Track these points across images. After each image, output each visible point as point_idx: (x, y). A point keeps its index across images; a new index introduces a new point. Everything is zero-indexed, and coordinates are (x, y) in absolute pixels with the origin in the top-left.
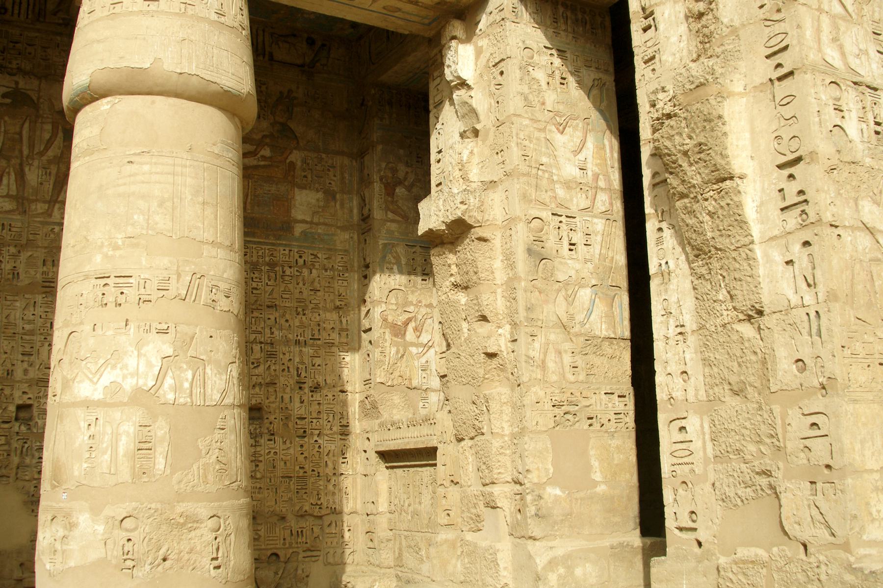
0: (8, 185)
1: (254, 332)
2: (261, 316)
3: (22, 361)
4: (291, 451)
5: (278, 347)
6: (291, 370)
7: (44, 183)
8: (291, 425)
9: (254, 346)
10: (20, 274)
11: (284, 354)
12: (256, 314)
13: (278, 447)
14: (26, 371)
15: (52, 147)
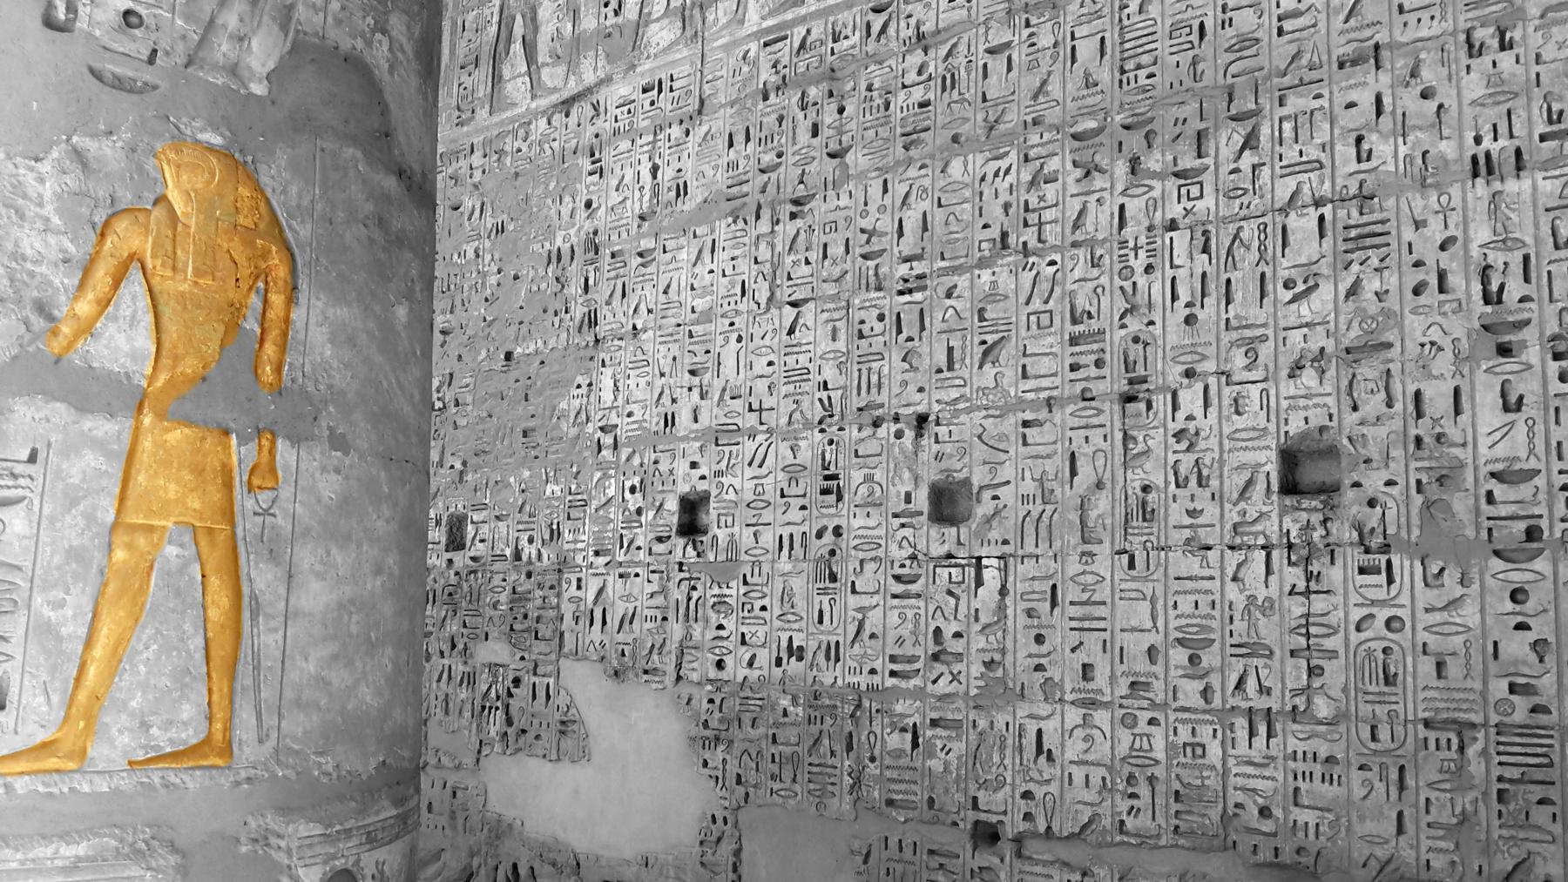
1: (1292, 170)
2: (1317, 104)
4: (1469, 614)
5: (1391, 202)
6: (1455, 280)
8: (1461, 505)
9: (1293, 221)
11: (1418, 225)
12: (1295, 103)
13: (1405, 599)
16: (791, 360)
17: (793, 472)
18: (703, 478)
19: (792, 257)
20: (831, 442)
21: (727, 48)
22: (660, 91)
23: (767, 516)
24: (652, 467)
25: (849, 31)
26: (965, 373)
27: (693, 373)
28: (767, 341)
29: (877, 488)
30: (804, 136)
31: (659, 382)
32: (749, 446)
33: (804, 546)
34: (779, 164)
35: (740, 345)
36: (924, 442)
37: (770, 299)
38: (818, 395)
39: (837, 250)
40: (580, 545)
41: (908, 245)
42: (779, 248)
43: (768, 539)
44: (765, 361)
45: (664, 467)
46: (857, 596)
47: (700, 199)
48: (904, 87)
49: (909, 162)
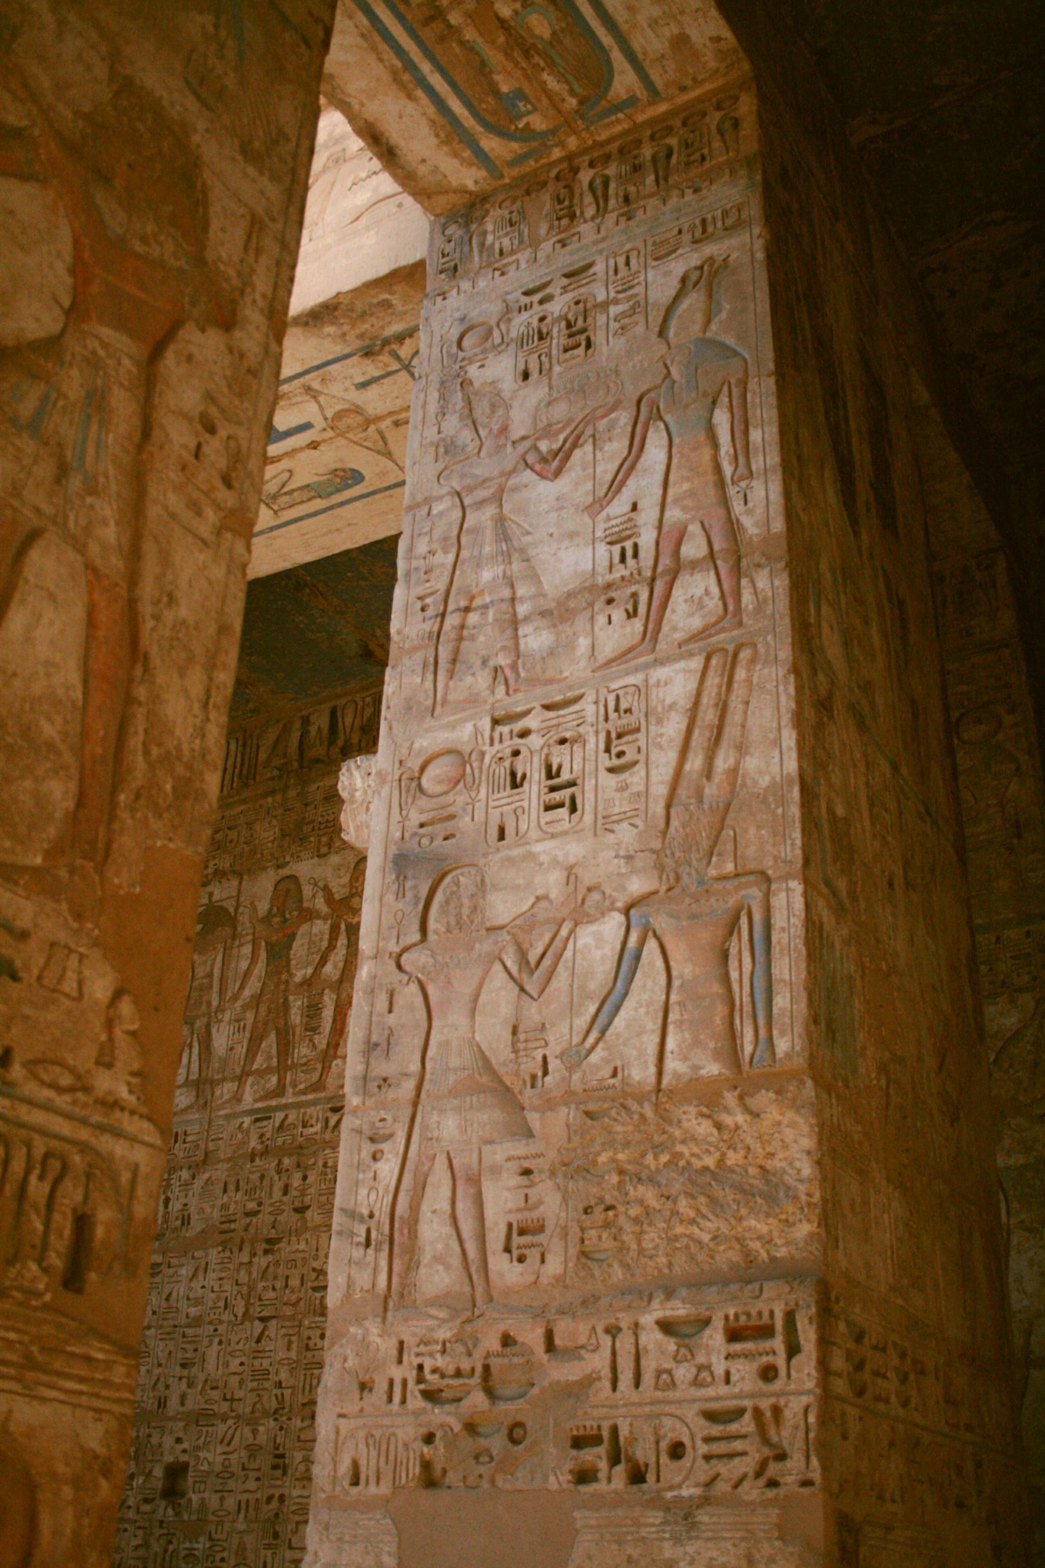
16: (257, 1362)
17: (253, 1450)
19: (263, 1284)
21: (227, 1117)
23: (231, 1484)
25: (313, 1122)
27: (183, 1366)
28: (240, 1346)
30: (277, 1194)
31: (157, 1371)
32: (221, 1428)
33: (257, 1510)
34: (258, 1212)
37: (246, 1314)
38: (275, 1391)
39: (295, 1282)
42: (254, 1275)
43: (230, 1503)
44: (238, 1361)
45: (154, 1441)
47: (199, 1229)
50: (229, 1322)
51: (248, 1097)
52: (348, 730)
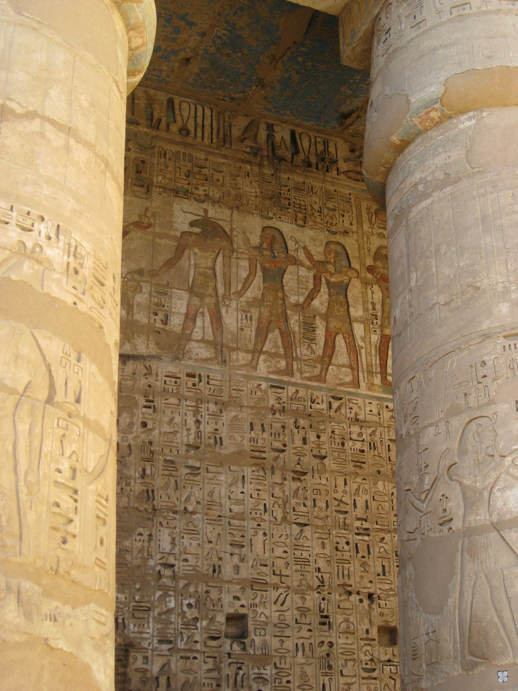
0: (203, 328)
3: (232, 554)
7: (245, 329)
10: (223, 439)
14: (237, 568)
15: (251, 288)
16: (298, 553)
17: (303, 611)
18: (243, 606)
20: (323, 599)
22: (200, 381)
23: (287, 632)
24: (205, 595)
26: (391, 578)
28: (283, 539)
29: (351, 625)
30: (298, 442)
32: (274, 594)
33: (312, 650)
34: (283, 451)
35: (265, 538)
36: (374, 606)
40: (144, 635)
41: (360, 512)
42: (287, 493)
43: (289, 644)
44: (282, 550)
46: (344, 678)
48: (351, 439)
49: (357, 475)
50: (271, 521)
51: (263, 368)
52: (307, 152)
